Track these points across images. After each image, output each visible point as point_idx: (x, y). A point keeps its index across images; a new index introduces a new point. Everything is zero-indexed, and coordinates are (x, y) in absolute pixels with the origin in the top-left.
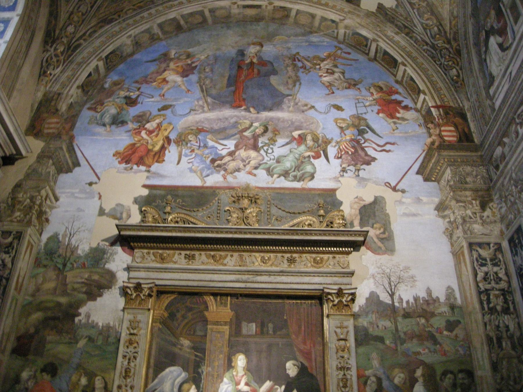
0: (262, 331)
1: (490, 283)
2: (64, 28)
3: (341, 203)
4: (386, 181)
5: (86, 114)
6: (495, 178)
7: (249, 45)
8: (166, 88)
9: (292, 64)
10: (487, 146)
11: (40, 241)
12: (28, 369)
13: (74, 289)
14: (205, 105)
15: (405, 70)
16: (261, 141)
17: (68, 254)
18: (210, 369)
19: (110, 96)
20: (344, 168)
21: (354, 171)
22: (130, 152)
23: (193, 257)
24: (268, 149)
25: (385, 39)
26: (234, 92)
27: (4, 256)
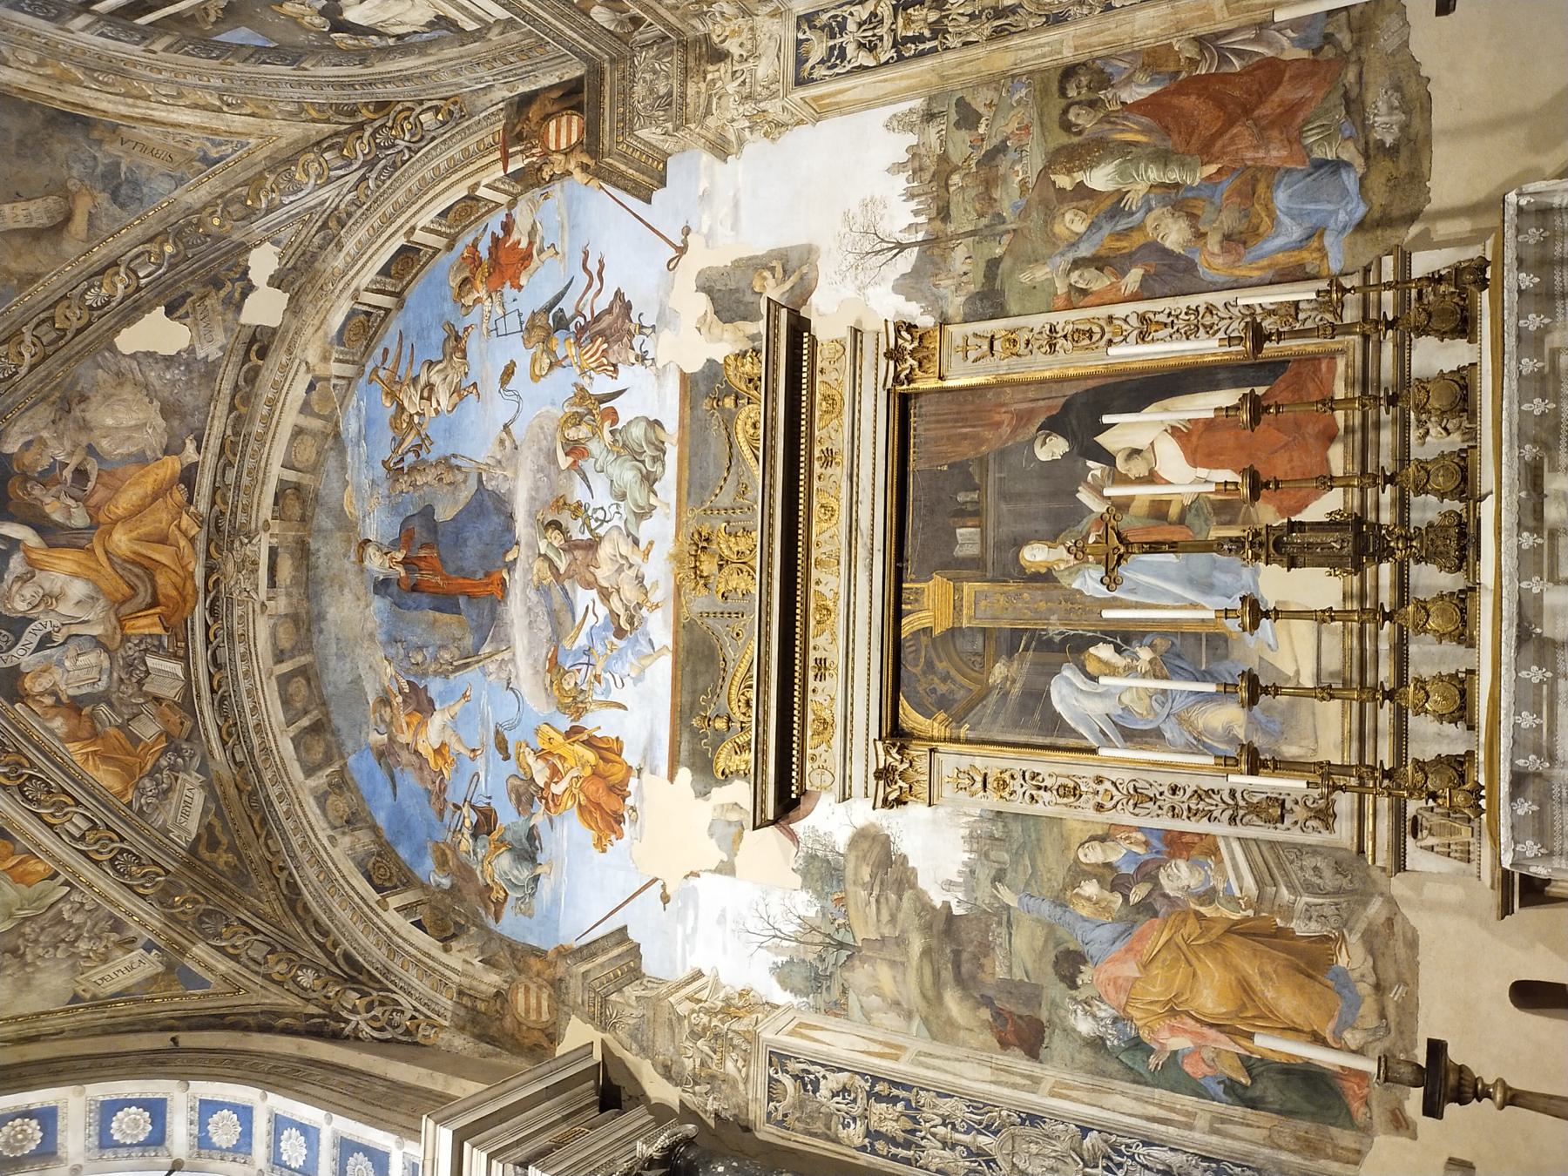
0: (974, 514)
1: (881, 38)
2: (303, 993)
3: (711, 362)
5: (510, 924)
6: (659, 28)
7: (362, 571)
8: (456, 747)
10: (591, 47)
11: (790, 1008)
12: (1072, 1018)
13: (893, 919)
14: (498, 657)
15: (424, 229)
16: (576, 535)
17: (818, 938)
18: (1054, 618)
19: (472, 872)
23: (821, 663)
25: (351, 273)
26: (470, 596)
27: (824, 1092)
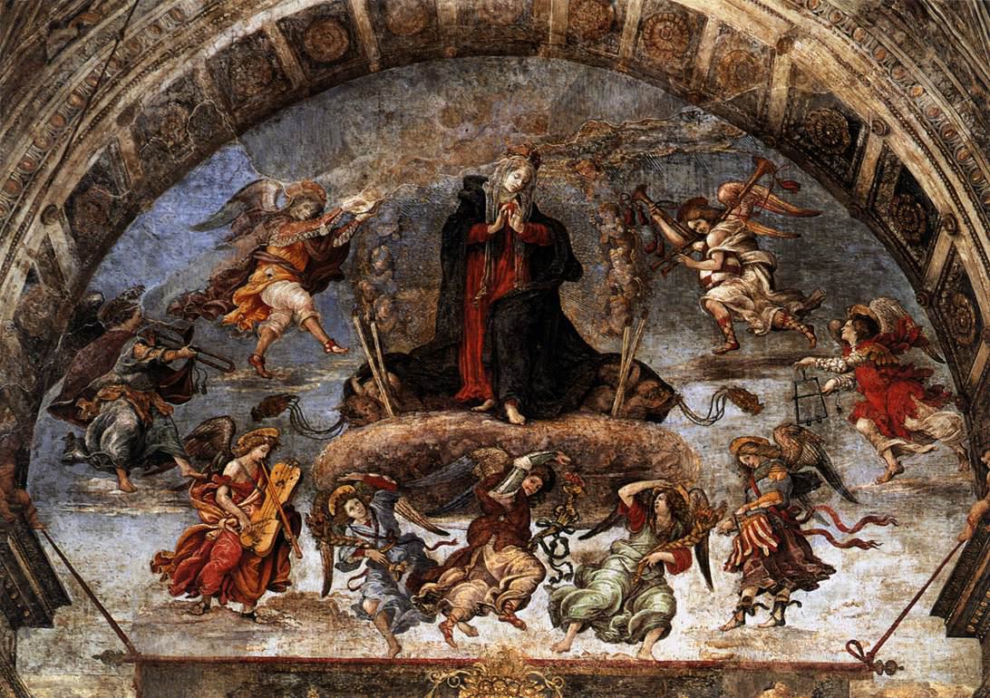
4: (849, 639)
5: (49, 432)
9: (626, 235)
15: (953, 252)
20: (748, 599)
21: (771, 605)
22: (193, 558)
24: (554, 545)
